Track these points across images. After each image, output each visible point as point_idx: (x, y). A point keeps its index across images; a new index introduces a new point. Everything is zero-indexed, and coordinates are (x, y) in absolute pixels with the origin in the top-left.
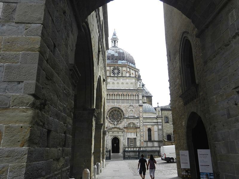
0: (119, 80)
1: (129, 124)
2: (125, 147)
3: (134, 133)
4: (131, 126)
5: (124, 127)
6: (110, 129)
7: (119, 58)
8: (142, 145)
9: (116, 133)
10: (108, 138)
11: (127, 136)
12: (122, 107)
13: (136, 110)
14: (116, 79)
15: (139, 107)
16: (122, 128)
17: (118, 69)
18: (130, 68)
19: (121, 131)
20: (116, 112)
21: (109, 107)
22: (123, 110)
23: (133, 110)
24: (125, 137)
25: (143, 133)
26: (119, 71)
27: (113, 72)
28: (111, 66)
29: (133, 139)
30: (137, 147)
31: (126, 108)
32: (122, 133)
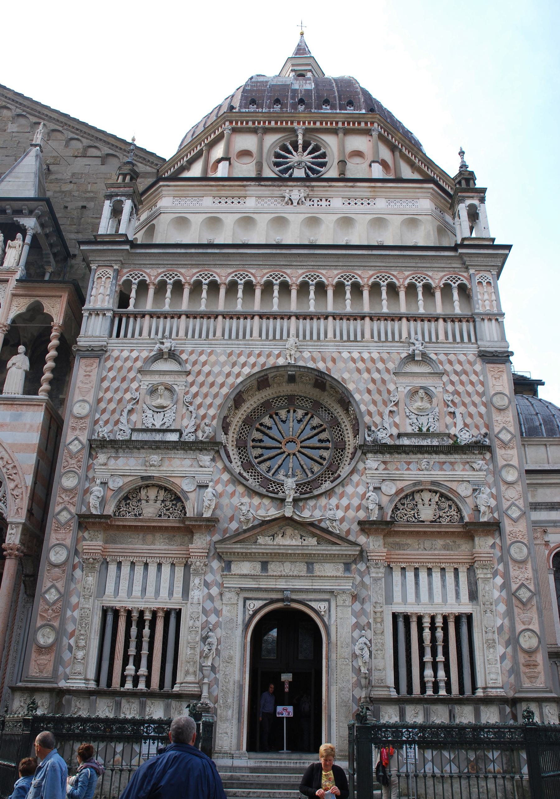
0: (324, 203)
2: (372, 700)
3: (450, 577)
5: (360, 523)
6: (237, 533)
7: (319, 97)
8: (532, 678)
9: (287, 568)
10: (218, 613)
11: (389, 600)
12: (340, 365)
13: (460, 388)
14: (297, 193)
15: (478, 367)
16: (345, 526)
17: (316, 148)
18: (393, 148)
19: (334, 550)
20: (300, 413)
21: (236, 370)
22: (351, 387)
24: (368, 607)
25: (529, 573)
26: (324, 155)
27: (277, 164)
28: (267, 131)
29: (439, 622)
30: (488, 701)
31: (376, 376)
32: (347, 567)
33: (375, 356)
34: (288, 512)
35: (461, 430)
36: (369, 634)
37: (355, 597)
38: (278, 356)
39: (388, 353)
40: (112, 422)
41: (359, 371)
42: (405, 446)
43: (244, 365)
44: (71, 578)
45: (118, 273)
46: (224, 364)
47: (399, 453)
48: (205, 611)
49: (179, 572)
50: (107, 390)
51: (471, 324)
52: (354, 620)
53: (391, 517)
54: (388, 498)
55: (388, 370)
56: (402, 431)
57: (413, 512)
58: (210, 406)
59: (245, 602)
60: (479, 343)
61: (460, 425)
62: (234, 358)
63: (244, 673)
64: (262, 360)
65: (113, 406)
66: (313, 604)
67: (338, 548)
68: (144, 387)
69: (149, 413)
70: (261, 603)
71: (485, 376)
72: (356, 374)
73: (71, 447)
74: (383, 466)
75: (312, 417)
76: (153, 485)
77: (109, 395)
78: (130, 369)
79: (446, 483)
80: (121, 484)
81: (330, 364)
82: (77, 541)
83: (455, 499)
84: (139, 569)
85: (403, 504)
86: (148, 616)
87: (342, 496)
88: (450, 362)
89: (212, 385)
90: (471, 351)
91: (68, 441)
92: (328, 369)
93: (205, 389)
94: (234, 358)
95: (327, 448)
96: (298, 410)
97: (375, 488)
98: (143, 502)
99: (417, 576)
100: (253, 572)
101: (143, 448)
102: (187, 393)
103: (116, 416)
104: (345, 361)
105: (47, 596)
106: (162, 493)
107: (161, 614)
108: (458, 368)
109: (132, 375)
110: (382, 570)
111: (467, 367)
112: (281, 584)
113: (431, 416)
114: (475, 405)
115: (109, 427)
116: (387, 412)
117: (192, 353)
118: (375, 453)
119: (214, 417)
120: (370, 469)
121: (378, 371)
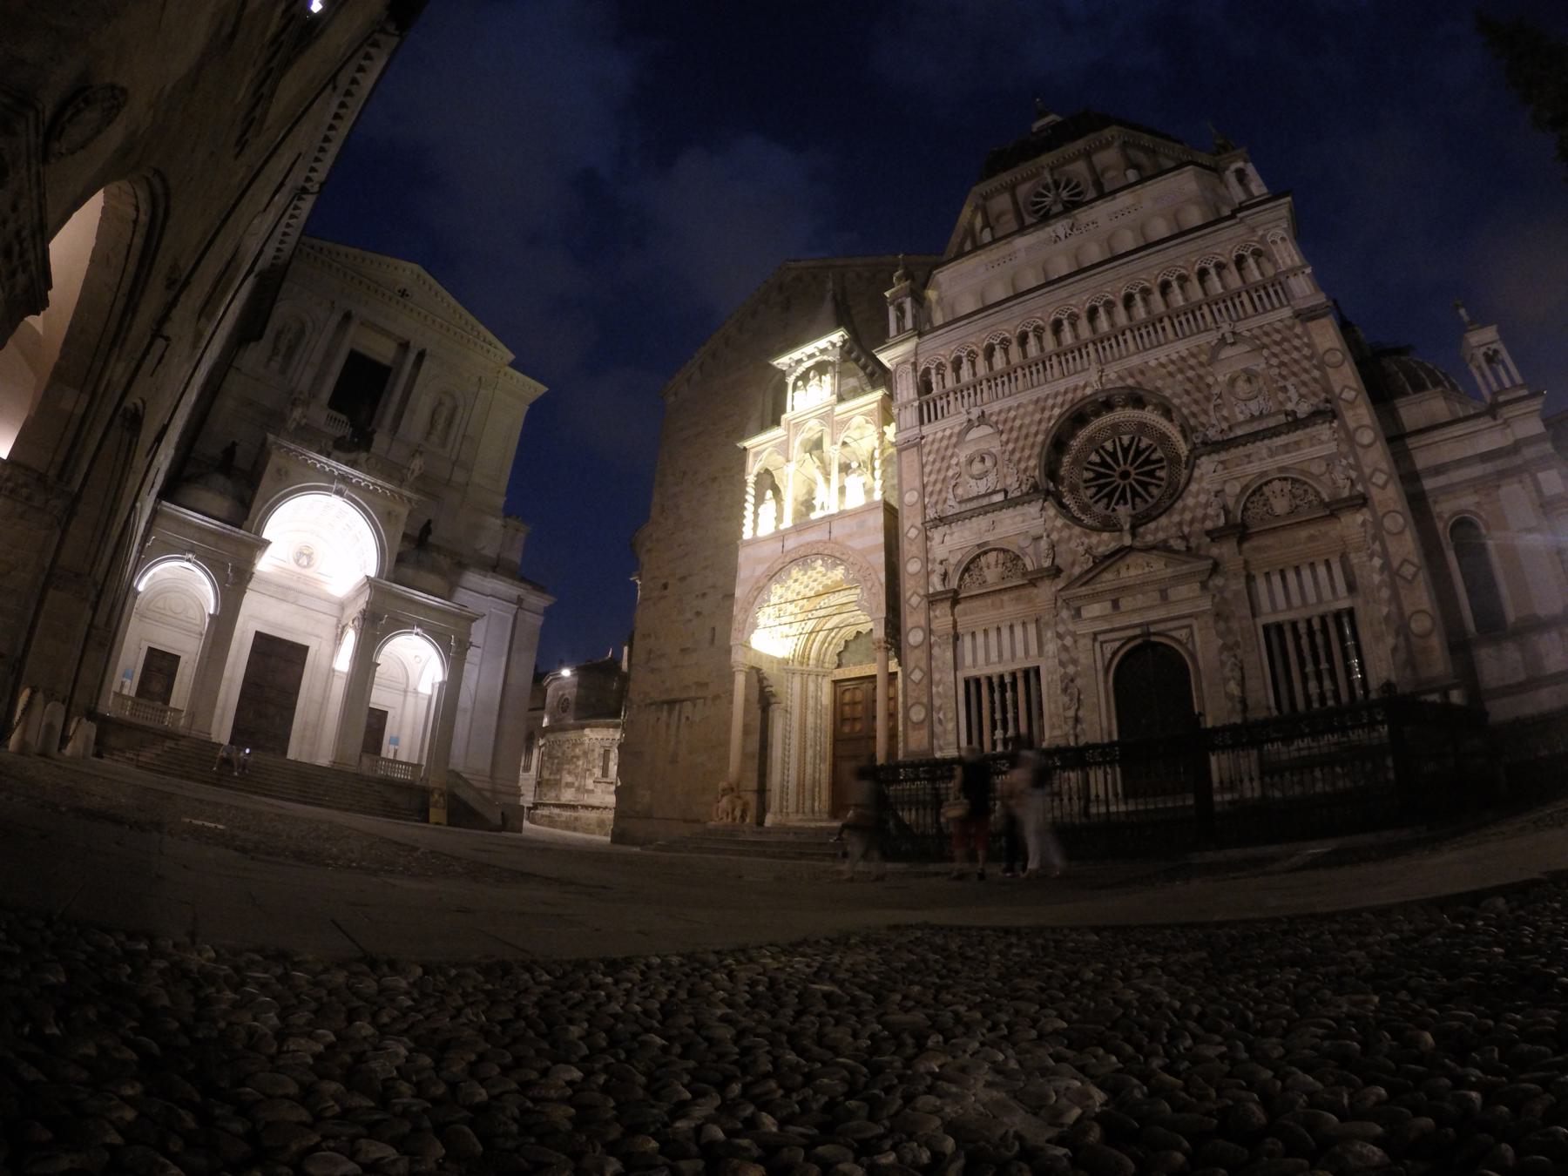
1: (1256, 491)
3: (1322, 571)
4: (1281, 506)
5: (1208, 533)
6: (1081, 576)
9: (1140, 601)
10: (1075, 662)
11: (1254, 613)
13: (1285, 358)
15: (1298, 330)
19: (1185, 568)
21: (1047, 414)
22: (1168, 393)
23: (1259, 365)
24: (1235, 625)
29: (1316, 624)
31: (1191, 374)
32: (1204, 586)
33: (1185, 353)
34: (1127, 541)
35: (1297, 403)
36: (1239, 652)
37: (1218, 616)
38: (1085, 386)
39: (1198, 346)
40: (941, 502)
41: (1171, 374)
42: (1241, 436)
43: (1053, 407)
44: (930, 657)
45: (915, 365)
46: (1033, 413)
47: (1237, 447)
48: (1062, 664)
49: (1032, 629)
50: (930, 474)
51: (1278, 288)
52: (1220, 642)
53: (1242, 519)
54: (1234, 499)
55: (1202, 364)
56: (1233, 422)
57: (1265, 509)
58: (1029, 457)
59: (1101, 647)
60: (1292, 303)
61: (1295, 397)
62: (1041, 404)
63: (1109, 719)
64: (1070, 396)
65: (939, 486)
66: (1174, 634)
67: (1188, 566)
68: (963, 460)
69: (973, 482)
70: (1117, 644)
71: (1310, 337)
72: (1169, 381)
73: (909, 535)
74: (1220, 467)
75: (1140, 440)
76: (991, 550)
77: (933, 477)
78: (947, 448)
79: (1295, 466)
80: (960, 557)
81: (1140, 378)
82: (929, 621)
83: (1308, 480)
84: (993, 635)
85: (1253, 503)
86: (1008, 679)
87: (1184, 509)
88: (1267, 334)
89: (1027, 436)
90: (1286, 312)
91: (905, 531)
92: (1138, 383)
93: (1021, 443)
94: (1041, 404)
95: (1163, 467)
96: (1123, 437)
97: (1217, 494)
98: (985, 569)
99: (1284, 579)
100: (1104, 613)
101: (972, 517)
102: (1004, 452)
103: (944, 495)
104: (1153, 369)
105: (913, 677)
106: (1001, 555)
107: (1019, 675)
108: (1277, 337)
109: (949, 452)
110: (1243, 580)
111: (1287, 333)
112: (1136, 619)
113: (1260, 398)
114: (1306, 371)
115: (939, 507)
116: (1212, 407)
117: (1000, 412)
118: (1209, 454)
119: (1035, 467)
120: (1208, 473)
121: (1192, 368)
